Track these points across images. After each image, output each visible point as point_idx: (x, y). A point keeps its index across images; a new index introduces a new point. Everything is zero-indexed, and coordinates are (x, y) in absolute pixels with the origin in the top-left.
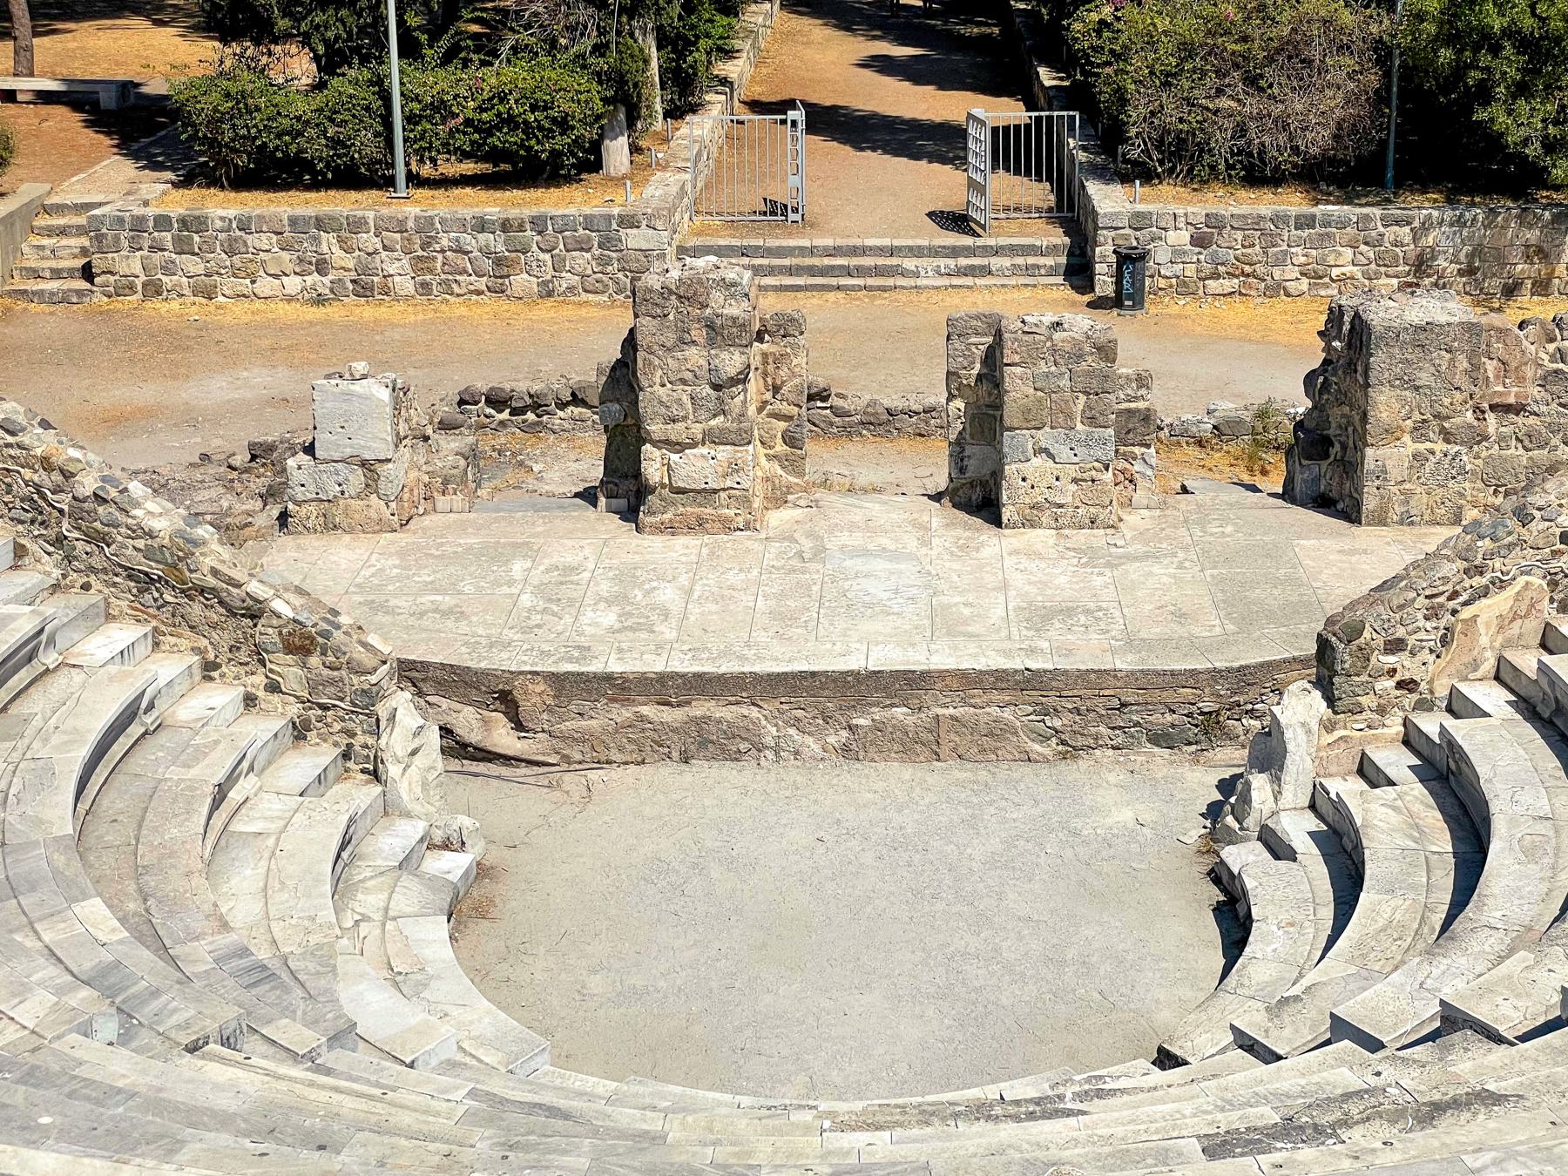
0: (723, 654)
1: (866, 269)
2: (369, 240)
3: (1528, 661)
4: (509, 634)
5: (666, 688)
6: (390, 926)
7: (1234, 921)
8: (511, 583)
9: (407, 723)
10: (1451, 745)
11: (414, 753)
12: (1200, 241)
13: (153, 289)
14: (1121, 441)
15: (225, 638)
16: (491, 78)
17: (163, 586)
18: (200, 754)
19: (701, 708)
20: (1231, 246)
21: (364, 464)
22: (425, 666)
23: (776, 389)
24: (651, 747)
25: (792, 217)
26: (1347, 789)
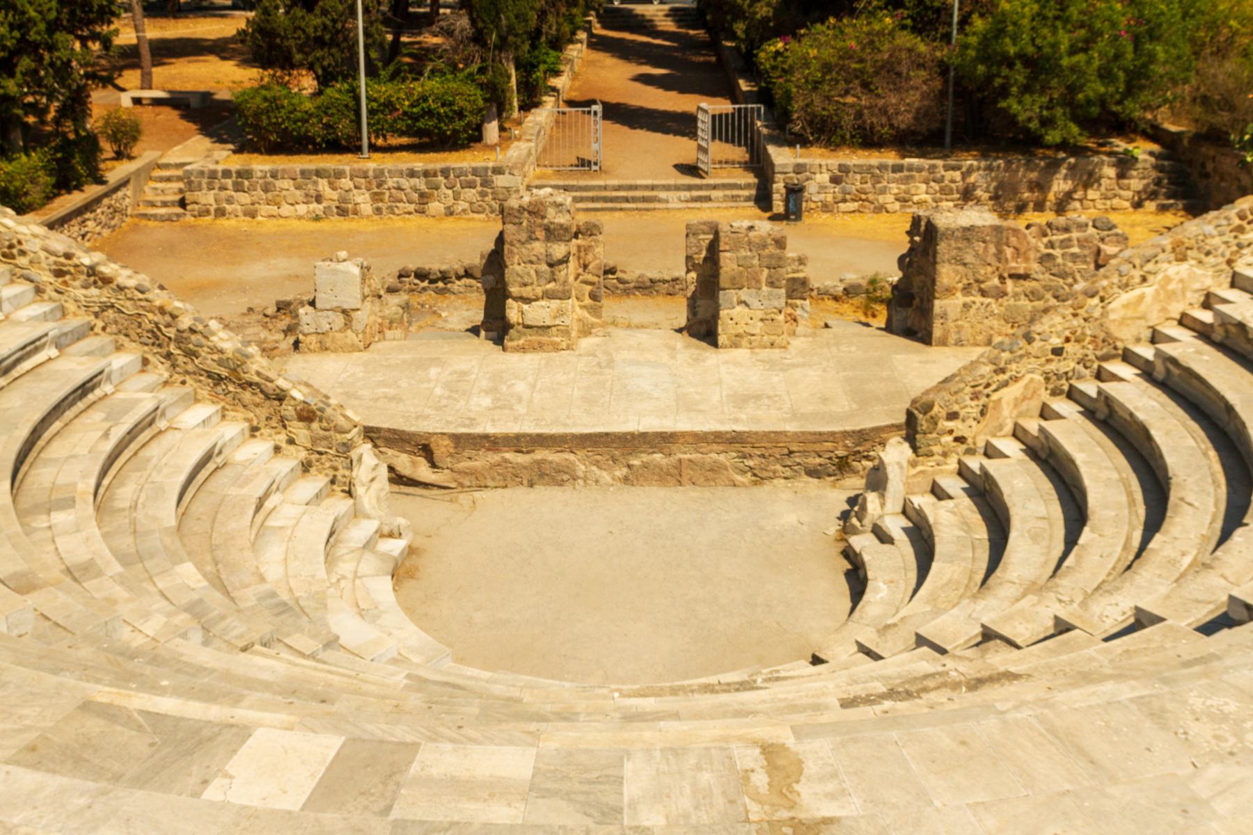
1: (639, 198)
2: (346, 183)
3: (1032, 425)
4: (428, 411)
5: (520, 443)
6: (358, 582)
7: (857, 580)
8: (429, 381)
9: (369, 464)
10: (986, 475)
11: (372, 480)
12: (835, 180)
13: (221, 213)
14: (789, 296)
15: (263, 412)
16: (417, 88)
17: (228, 381)
18: (248, 480)
19: (540, 454)
20: (854, 183)
21: (344, 312)
22: (378, 430)
23: (585, 267)
24: (511, 477)
25: (594, 168)
26: (923, 501)
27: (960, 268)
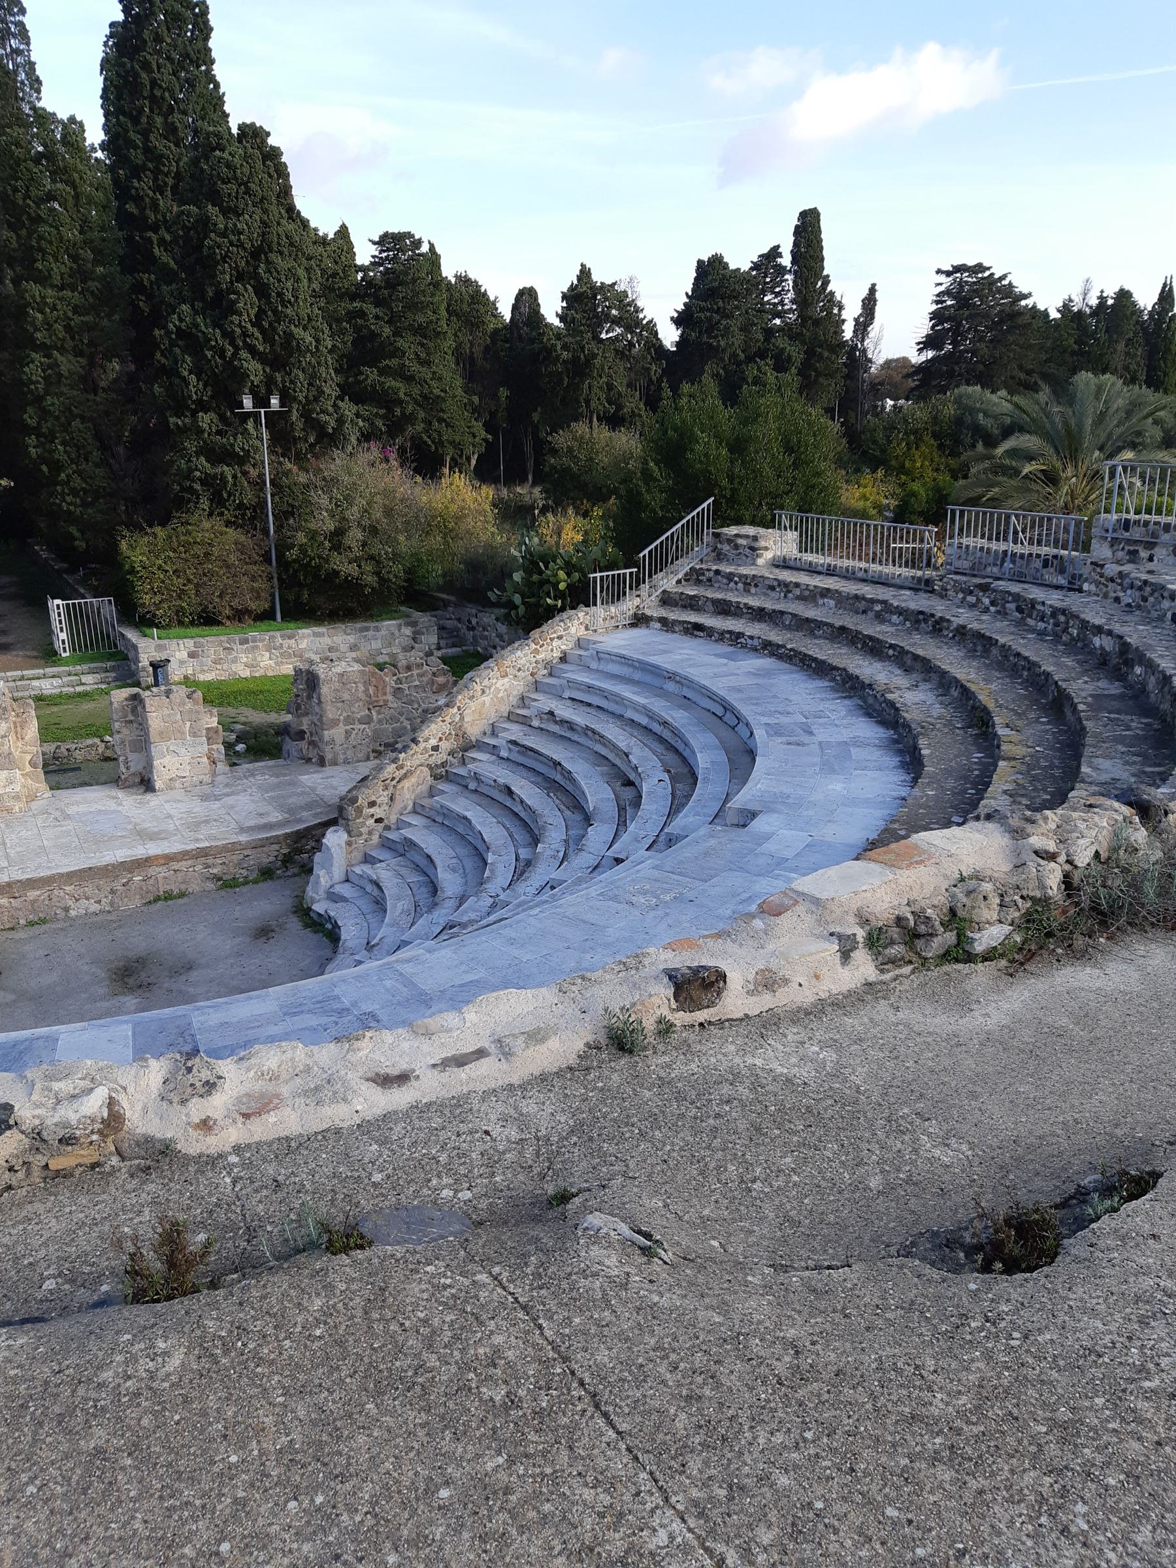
0: (39, 866)
3: (426, 802)
27: (340, 705)
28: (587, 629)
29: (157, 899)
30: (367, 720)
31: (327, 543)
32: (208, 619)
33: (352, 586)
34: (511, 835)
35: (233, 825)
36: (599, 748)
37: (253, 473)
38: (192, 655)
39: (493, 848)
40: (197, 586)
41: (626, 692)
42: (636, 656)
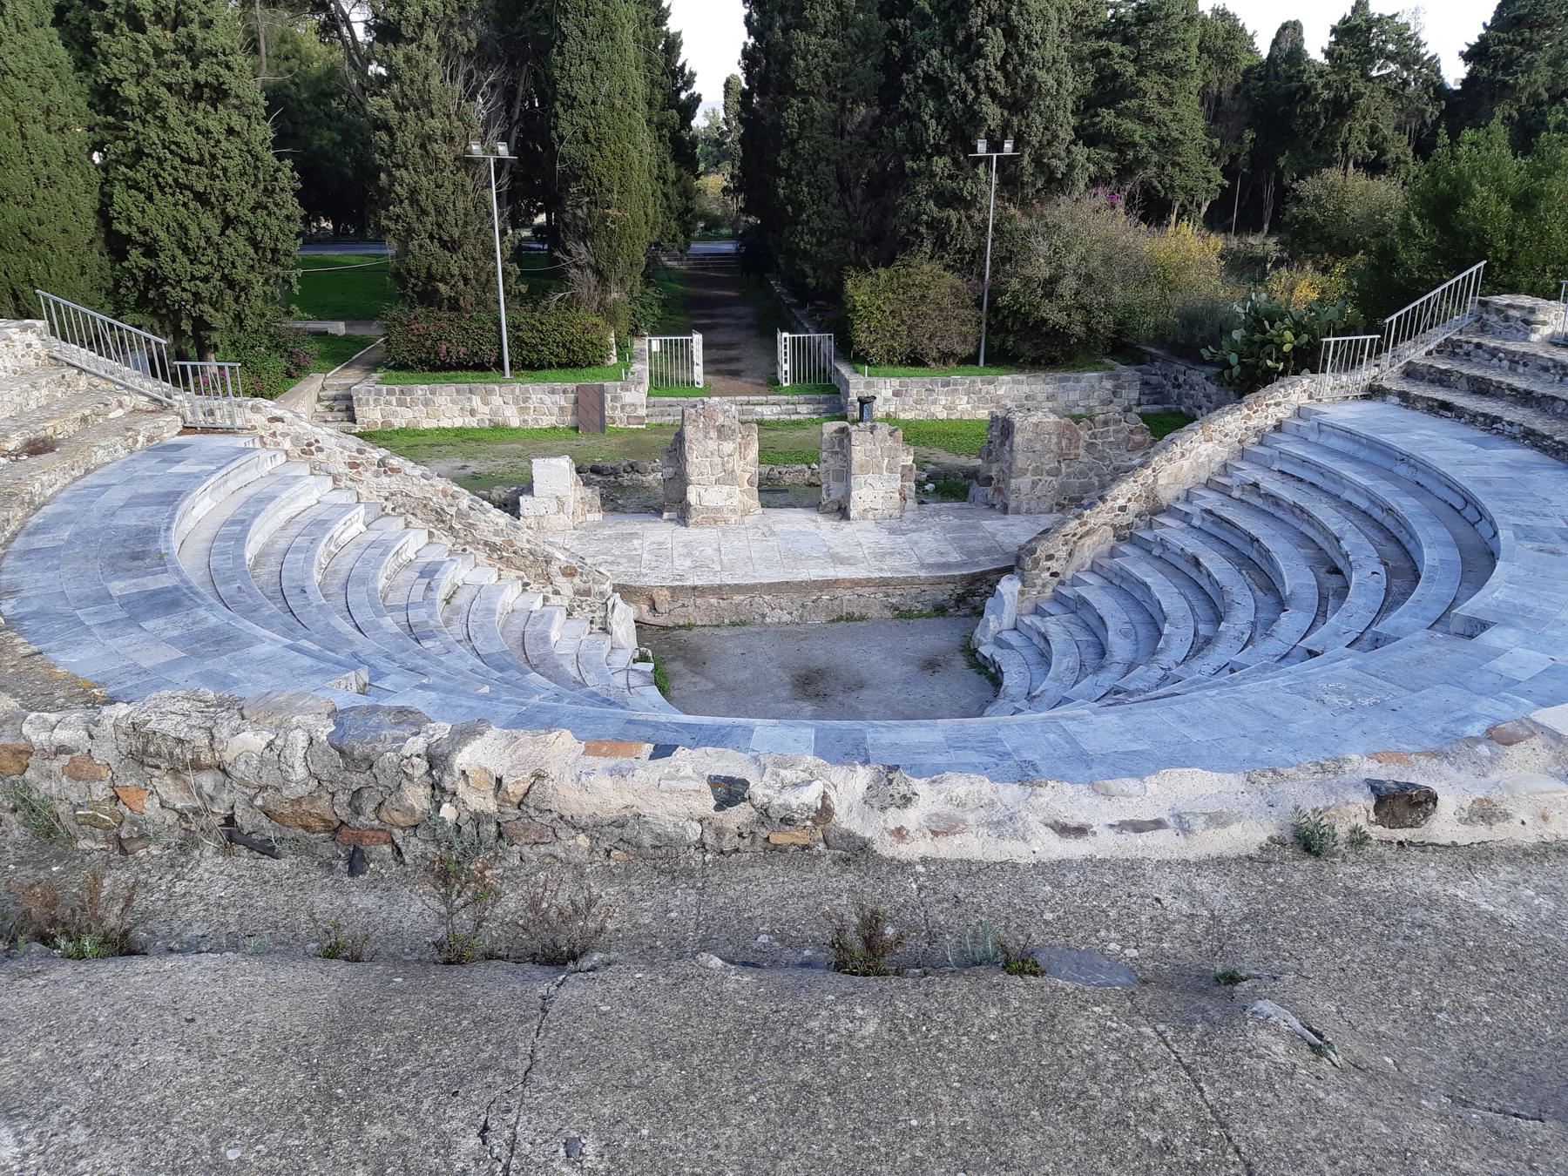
0: (746, 575)
3: (1106, 562)
4: (644, 571)
28: (1310, 397)
29: (840, 619)
30: (1056, 473)
31: (1040, 291)
32: (916, 360)
33: (1058, 335)
34: (1192, 609)
35: (915, 560)
36: (1305, 528)
37: (978, 218)
38: (896, 394)
39: (1171, 618)
40: (910, 328)
41: (1348, 471)
42: (1364, 432)
